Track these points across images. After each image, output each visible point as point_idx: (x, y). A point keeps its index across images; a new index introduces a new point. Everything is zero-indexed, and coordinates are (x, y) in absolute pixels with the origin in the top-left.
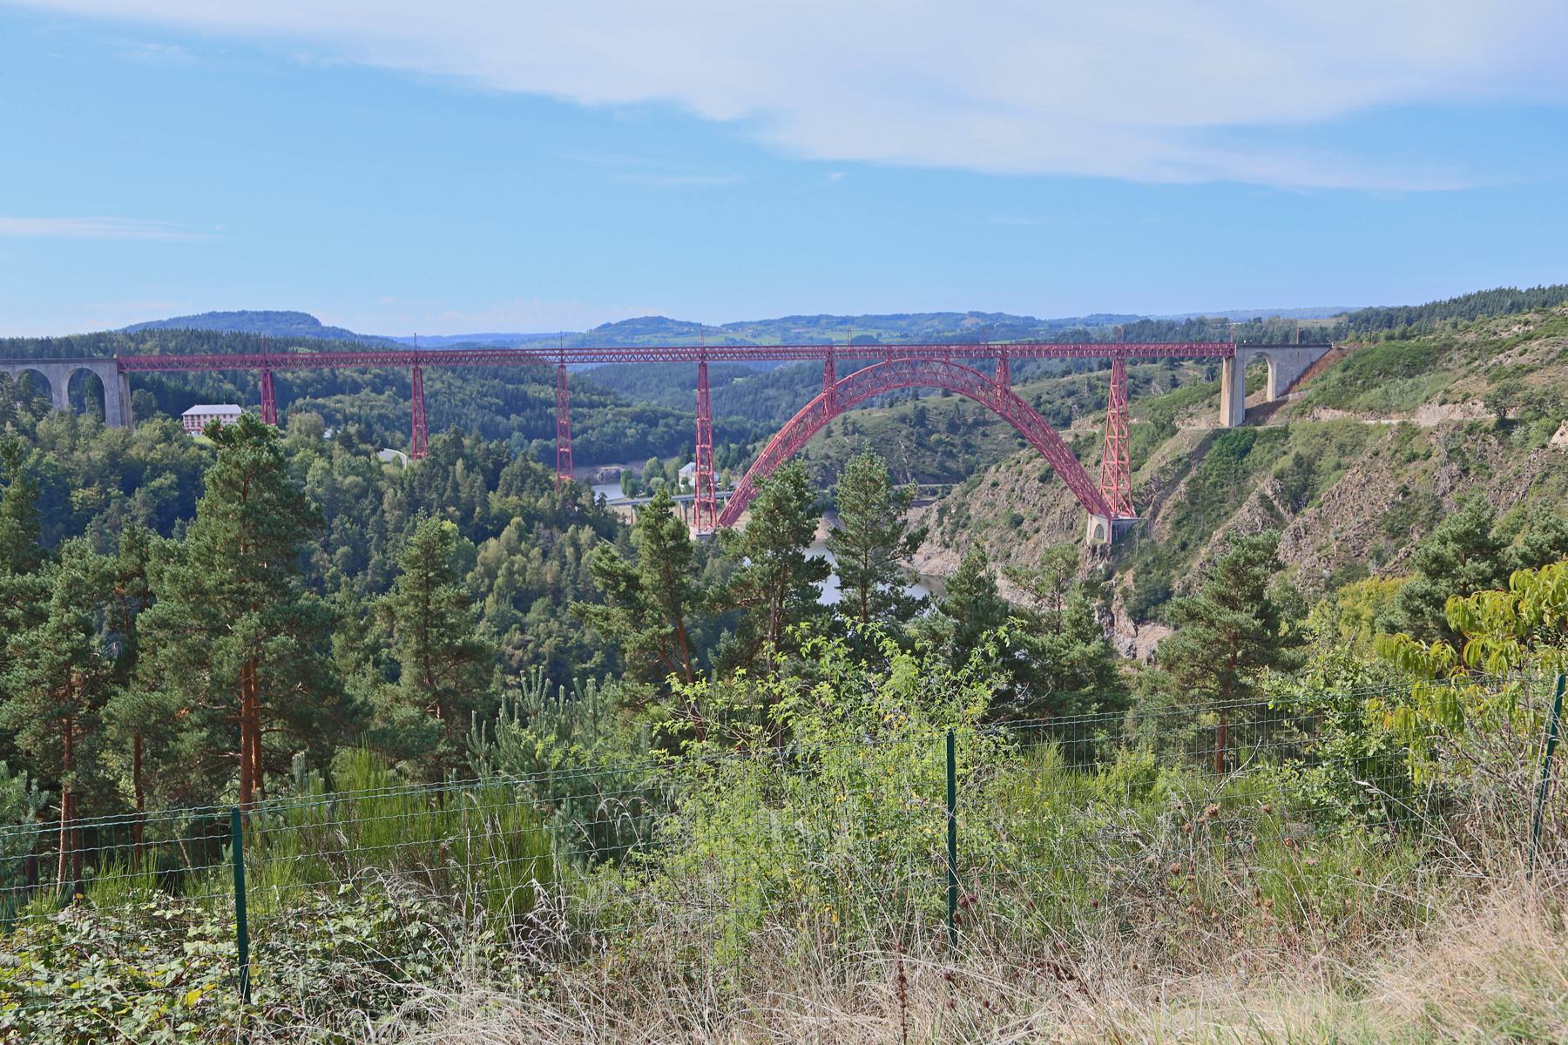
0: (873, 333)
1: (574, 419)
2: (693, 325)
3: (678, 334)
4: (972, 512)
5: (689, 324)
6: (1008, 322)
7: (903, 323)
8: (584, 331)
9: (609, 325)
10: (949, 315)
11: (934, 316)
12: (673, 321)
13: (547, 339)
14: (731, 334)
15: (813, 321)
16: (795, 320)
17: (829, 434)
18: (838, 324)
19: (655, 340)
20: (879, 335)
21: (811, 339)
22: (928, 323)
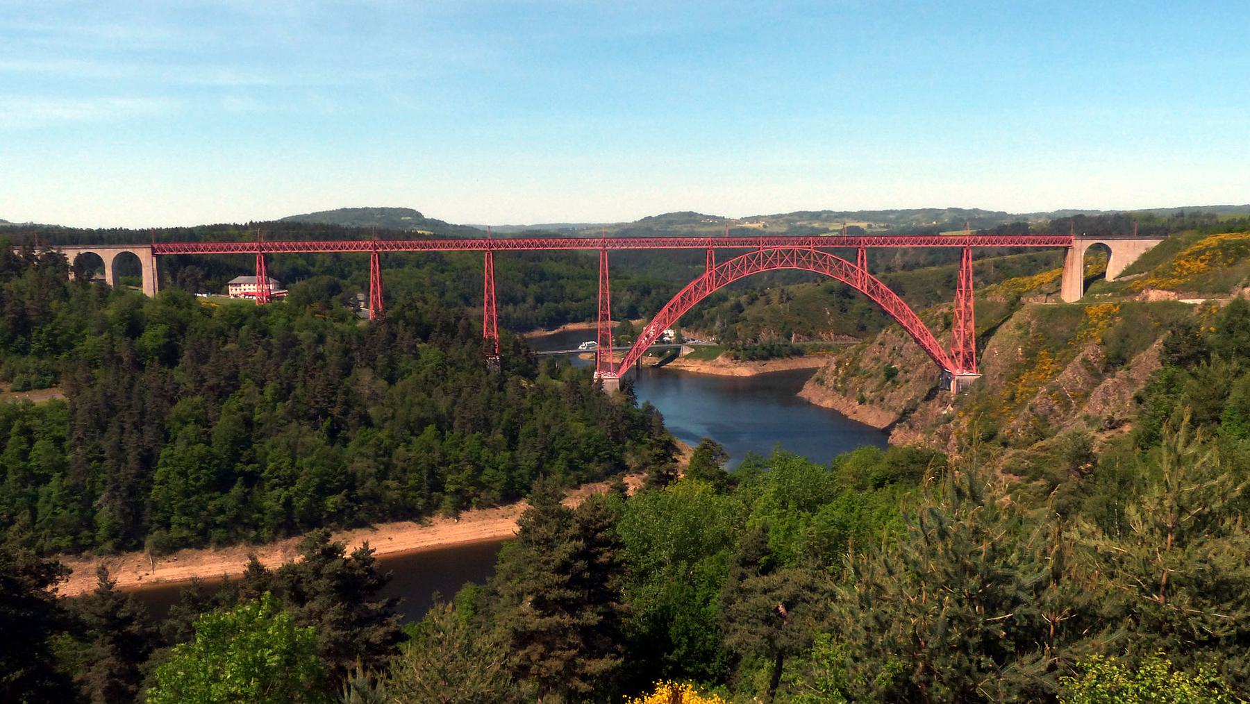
0: (863, 225)
1: (580, 288)
2: (717, 218)
3: (705, 224)
4: (862, 365)
5: (714, 217)
6: (982, 216)
7: (891, 216)
8: (630, 220)
9: (650, 217)
10: (931, 210)
11: (918, 211)
12: (701, 215)
13: (601, 228)
14: (747, 225)
15: (816, 216)
16: (801, 215)
17: (768, 302)
18: (836, 217)
19: (685, 229)
20: (870, 226)
21: (813, 228)
22: (913, 217)
